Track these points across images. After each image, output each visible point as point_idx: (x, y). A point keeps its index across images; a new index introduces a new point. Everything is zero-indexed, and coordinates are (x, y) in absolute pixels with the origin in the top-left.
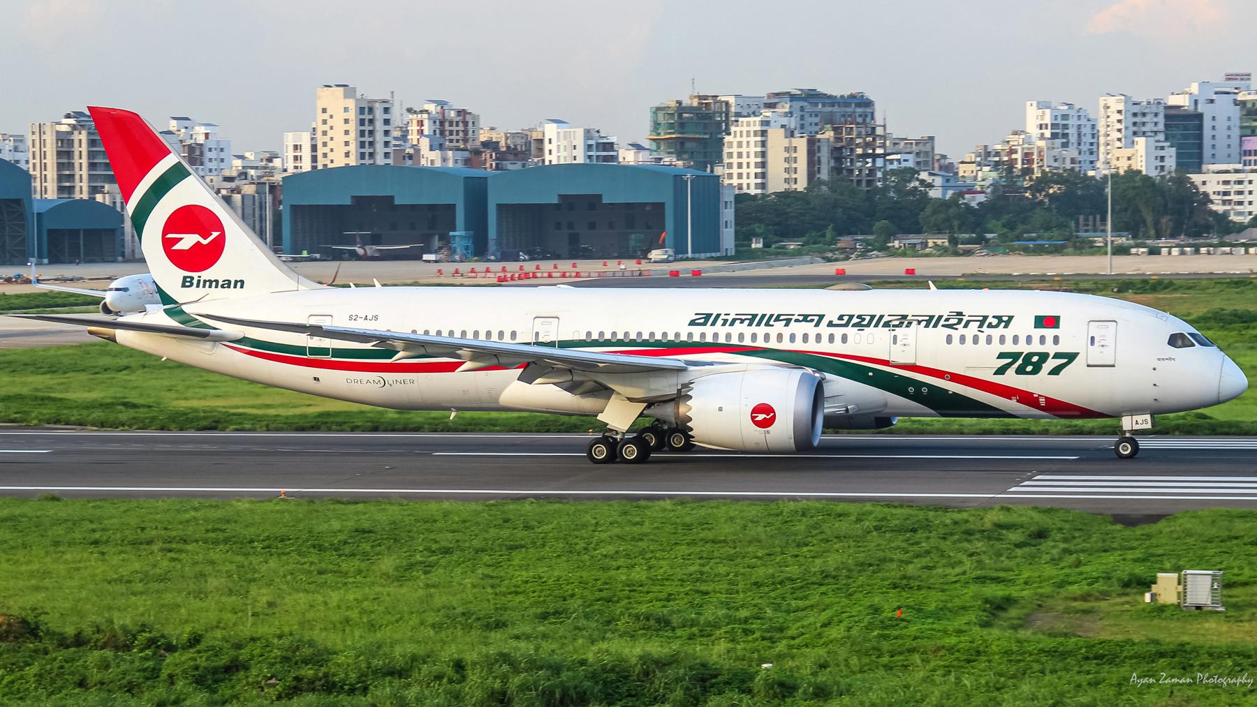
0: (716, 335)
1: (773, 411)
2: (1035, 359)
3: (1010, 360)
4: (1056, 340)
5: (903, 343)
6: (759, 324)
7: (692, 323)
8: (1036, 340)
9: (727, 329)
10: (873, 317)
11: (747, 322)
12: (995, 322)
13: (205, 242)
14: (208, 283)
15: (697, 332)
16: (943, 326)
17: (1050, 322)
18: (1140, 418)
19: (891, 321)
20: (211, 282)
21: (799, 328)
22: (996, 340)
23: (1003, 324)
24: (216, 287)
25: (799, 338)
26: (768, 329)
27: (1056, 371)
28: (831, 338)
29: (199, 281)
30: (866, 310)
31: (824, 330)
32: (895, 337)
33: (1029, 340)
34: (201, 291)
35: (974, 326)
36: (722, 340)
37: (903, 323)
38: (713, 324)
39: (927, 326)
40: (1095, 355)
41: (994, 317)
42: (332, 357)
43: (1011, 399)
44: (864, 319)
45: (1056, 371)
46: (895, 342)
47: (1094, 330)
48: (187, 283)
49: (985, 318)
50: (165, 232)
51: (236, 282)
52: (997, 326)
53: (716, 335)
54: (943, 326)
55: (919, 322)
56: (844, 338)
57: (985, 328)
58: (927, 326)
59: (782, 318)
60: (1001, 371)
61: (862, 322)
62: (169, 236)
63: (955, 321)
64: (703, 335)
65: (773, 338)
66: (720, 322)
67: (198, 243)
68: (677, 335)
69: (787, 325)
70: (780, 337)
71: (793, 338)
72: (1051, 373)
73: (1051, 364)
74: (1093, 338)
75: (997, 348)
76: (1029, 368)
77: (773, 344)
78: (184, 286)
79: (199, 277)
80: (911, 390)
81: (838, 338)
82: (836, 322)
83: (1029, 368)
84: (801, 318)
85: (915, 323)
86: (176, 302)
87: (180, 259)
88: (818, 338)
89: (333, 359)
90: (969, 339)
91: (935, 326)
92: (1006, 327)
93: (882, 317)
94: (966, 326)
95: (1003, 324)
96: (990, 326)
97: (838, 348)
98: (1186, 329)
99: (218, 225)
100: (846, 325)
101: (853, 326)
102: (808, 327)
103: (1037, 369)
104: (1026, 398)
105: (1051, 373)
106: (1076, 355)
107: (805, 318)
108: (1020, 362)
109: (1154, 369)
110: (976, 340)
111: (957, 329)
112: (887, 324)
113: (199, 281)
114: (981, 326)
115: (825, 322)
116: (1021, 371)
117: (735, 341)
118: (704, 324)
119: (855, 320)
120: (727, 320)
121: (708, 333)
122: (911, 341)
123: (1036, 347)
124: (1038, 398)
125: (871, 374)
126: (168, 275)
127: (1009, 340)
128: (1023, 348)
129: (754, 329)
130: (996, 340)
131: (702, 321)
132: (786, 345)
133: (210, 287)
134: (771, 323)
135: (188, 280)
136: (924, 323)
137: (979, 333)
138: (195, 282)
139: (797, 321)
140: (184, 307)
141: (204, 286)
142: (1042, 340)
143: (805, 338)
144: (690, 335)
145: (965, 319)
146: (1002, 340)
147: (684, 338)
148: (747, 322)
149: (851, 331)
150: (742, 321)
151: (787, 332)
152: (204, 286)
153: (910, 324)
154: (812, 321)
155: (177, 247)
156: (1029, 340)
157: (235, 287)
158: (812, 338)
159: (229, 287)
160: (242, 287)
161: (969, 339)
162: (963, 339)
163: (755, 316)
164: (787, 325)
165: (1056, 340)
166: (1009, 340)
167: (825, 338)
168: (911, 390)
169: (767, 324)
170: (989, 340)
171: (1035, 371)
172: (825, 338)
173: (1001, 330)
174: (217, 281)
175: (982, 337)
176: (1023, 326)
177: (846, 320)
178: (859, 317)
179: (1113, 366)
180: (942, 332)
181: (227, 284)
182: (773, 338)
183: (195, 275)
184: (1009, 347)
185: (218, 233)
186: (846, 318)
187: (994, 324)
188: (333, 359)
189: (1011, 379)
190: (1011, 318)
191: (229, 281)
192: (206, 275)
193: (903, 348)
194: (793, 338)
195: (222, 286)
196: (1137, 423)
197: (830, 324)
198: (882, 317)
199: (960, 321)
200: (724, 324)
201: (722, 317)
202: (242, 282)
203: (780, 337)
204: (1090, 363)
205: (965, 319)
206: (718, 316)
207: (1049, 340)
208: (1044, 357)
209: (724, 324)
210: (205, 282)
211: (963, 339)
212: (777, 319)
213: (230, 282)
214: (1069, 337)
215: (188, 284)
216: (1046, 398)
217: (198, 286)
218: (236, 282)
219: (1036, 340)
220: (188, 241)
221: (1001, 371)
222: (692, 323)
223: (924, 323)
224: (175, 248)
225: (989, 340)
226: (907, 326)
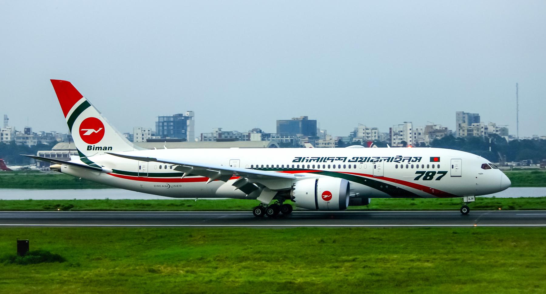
0: (303, 166)
1: (331, 195)
2: (430, 174)
3: (421, 174)
4: (439, 166)
5: (378, 168)
6: (321, 161)
7: (294, 161)
8: (431, 166)
9: (308, 163)
10: (366, 158)
11: (316, 161)
12: (414, 159)
13: (96, 132)
14: (97, 148)
15: (296, 165)
16: (394, 161)
17: (437, 159)
18: (470, 197)
19: (373, 160)
20: (99, 148)
22: (415, 166)
23: (418, 160)
24: (101, 150)
25: (337, 167)
26: (324, 163)
27: (439, 179)
28: (350, 167)
29: (94, 148)
31: (347, 163)
32: (375, 166)
33: (428, 166)
35: (406, 161)
36: (306, 168)
37: (378, 160)
38: (302, 161)
39: (388, 161)
40: (454, 172)
41: (414, 158)
42: (148, 176)
43: (421, 190)
44: (363, 159)
45: (439, 179)
46: (375, 168)
48: (89, 148)
49: (411, 158)
50: (81, 128)
51: (109, 148)
52: (415, 161)
53: (303, 166)
54: (394, 161)
55: (385, 160)
56: (355, 167)
57: (411, 162)
58: (388, 161)
59: (330, 159)
60: (417, 179)
62: (82, 130)
63: (399, 159)
64: (298, 166)
66: (305, 160)
68: (288, 166)
69: (332, 161)
70: (329, 167)
71: (334, 167)
72: (436, 180)
73: (436, 176)
74: (453, 166)
75: (415, 169)
76: (428, 178)
77: (326, 169)
78: (88, 149)
79: (94, 146)
81: (352, 167)
82: (352, 160)
83: (428, 178)
84: (338, 159)
85: (383, 160)
86: (85, 156)
87: (86, 139)
88: (345, 167)
90: (404, 167)
91: (391, 161)
92: (419, 161)
93: (370, 158)
94: (403, 161)
95: (418, 160)
96: (413, 161)
97: (352, 170)
98: (487, 162)
100: (356, 161)
101: (359, 161)
102: (341, 163)
103: (431, 178)
105: (436, 180)
106: (447, 172)
107: (339, 159)
108: (424, 175)
109: (476, 178)
110: (407, 167)
111: (400, 162)
112: (372, 161)
113: (94, 148)
114: (409, 161)
115: (347, 160)
116: (425, 179)
117: (311, 168)
118: (299, 161)
119: (359, 159)
120: (308, 160)
121: (301, 164)
122: (381, 168)
123: (431, 169)
126: (82, 146)
127: (420, 166)
128: (426, 170)
129: (319, 163)
130: (415, 166)
131: (298, 160)
132: (332, 170)
133: (98, 150)
134: (326, 161)
135: (90, 147)
136: (387, 160)
137: (408, 164)
138: (92, 148)
140: (88, 158)
141: (96, 150)
142: (433, 166)
143: (339, 167)
144: (293, 166)
145: (403, 158)
146: (418, 166)
147: (290, 167)
148: (316, 161)
149: (357, 164)
150: (314, 160)
151: (332, 165)
152: (96, 150)
153: (381, 161)
154: (342, 160)
155: (85, 134)
156: (428, 166)
158: (342, 167)
160: (111, 150)
161: (404, 167)
162: (402, 167)
164: (332, 161)
165: (439, 166)
166: (420, 166)
167: (347, 167)
168: (381, 187)
169: (324, 161)
170: (412, 167)
172: (347, 167)
173: (417, 163)
174: (101, 148)
175: (410, 166)
176: (425, 161)
177: (356, 159)
178: (361, 158)
179: (461, 176)
180: (394, 164)
181: (105, 148)
183: (92, 145)
184: (420, 169)
185: (102, 128)
186: (355, 159)
187: (414, 160)
189: (421, 182)
190: (421, 158)
191: (106, 148)
192: (97, 145)
194: (334, 167)
195: (103, 150)
196: (469, 199)
197: (349, 161)
198: (370, 158)
199: (401, 159)
200: (307, 161)
201: (306, 159)
202: (111, 148)
203: (329, 167)
204: (452, 175)
205: (403, 158)
206: (304, 158)
207: (436, 166)
208: (434, 173)
209: (307, 161)
210: (96, 148)
211: (402, 167)
212: (328, 159)
213: (106, 148)
214: (444, 166)
215: (89, 149)
216: (435, 189)
217: (93, 150)
218: (109, 148)
219: (431, 166)
220: (89, 132)
222: (294, 161)
225: (412, 167)
226: (380, 162)
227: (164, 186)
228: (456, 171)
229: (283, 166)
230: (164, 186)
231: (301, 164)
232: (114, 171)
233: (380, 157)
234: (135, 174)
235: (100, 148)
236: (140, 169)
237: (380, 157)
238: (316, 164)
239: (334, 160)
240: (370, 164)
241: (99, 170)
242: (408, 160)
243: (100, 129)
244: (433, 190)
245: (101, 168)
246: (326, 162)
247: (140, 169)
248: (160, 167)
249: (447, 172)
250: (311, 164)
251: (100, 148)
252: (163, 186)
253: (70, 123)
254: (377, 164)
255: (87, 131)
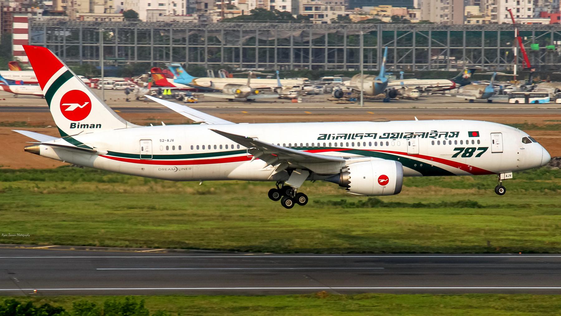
0: (330, 144)
2: (470, 150)
3: (459, 151)
4: (479, 142)
5: (413, 145)
6: (349, 138)
7: (319, 139)
8: (470, 142)
9: (335, 141)
10: (398, 134)
12: (452, 135)
13: (81, 107)
14: (83, 126)
16: (430, 137)
19: (406, 135)
20: (84, 125)
21: (367, 140)
22: (453, 142)
23: (455, 136)
24: (87, 127)
25: (367, 144)
26: (353, 141)
27: (479, 155)
28: (382, 144)
29: (78, 125)
30: (395, 131)
31: (378, 140)
32: (409, 142)
34: (80, 130)
35: (443, 137)
36: (333, 146)
38: (329, 139)
39: (423, 137)
40: (495, 148)
41: (451, 132)
42: (153, 159)
44: (395, 135)
45: (479, 155)
46: (409, 145)
47: (493, 137)
49: (447, 133)
50: (61, 103)
51: (97, 125)
52: (453, 136)
53: (330, 144)
54: (430, 137)
56: (387, 144)
58: (423, 137)
59: (358, 135)
60: (455, 156)
61: (394, 136)
63: (435, 135)
64: (324, 144)
65: (356, 144)
66: (331, 138)
67: (78, 107)
68: (313, 144)
69: (361, 138)
70: (359, 144)
71: (364, 144)
73: (477, 152)
74: (493, 141)
75: (454, 146)
76: (468, 155)
77: (356, 147)
78: (71, 127)
79: (79, 123)
80: (415, 165)
81: (384, 144)
82: (383, 136)
83: (468, 155)
84: (367, 135)
85: (417, 136)
88: (376, 144)
89: (153, 160)
90: (442, 143)
91: (426, 137)
92: (457, 137)
93: (402, 134)
94: (440, 137)
95: (455, 136)
96: (450, 136)
97: (384, 148)
99: (88, 99)
100: (388, 138)
101: (391, 138)
102: (371, 139)
104: (464, 167)
106: (487, 148)
107: (369, 135)
108: (464, 152)
109: (518, 153)
110: (444, 143)
111: (436, 138)
112: (405, 137)
113: (78, 125)
114: (446, 136)
115: (378, 137)
116: (464, 156)
117: (339, 146)
118: (325, 139)
119: (391, 136)
121: (327, 142)
122: (416, 144)
123: (470, 145)
124: (469, 167)
125: (399, 159)
126: (63, 123)
127: (459, 142)
128: (465, 146)
129: (347, 140)
130: (453, 142)
131: (323, 137)
132: (362, 148)
133: (84, 127)
134: (354, 137)
135: (73, 125)
137: (446, 140)
138: (77, 126)
139: (365, 136)
141: (81, 127)
143: (370, 144)
144: (319, 144)
146: (456, 142)
147: (316, 145)
149: (390, 140)
150: (341, 137)
151: (362, 142)
152: (81, 127)
153: (415, 137)
155: (67, 110)
157: (97, 127)
158: (373, 144)
159: (94, 127)
160: (100, 127)
161: (442, 143)
163: (346, 135)
164: (361, 138)
166: (459, 142)
167: (379, 144)
169: (353, 138)
170: (450, 143)
171: (470, 156)
172: (379, 144)
173: (454, 138)
174: (88, 125)
175: (447, 142)
176: (464, 136)
178: (392, 134)
179: (502, 152)
180: (430, 140)
182: (356, 144)
183: (77, 122)
184: (459, 146)
185: (88, 103)
186: (387, 135)
188: (153, 160)
189: (460, 159)
190: (458, 133)
191: (94, 125)
192: (82, 122)
193: (413, 147)
194: (364, 144)
195: (90, 127)
197: (380, 137)
198: (402, 134)
199: (437, 135)
201: (332, 135)
202: (100, 125)
203: (359, 144)
204: (493, 151)
206: (330, 135)
207: (476, 142)
208: (474, 149)
209: (333, 139)
210: (82, 125)
212: (357, 136)
213: (94, 125)
214: (484, 140)
215: (73, 127)
216: (473, 167)
217: (78, 127)
218: (97, 125)
219: (470, 142)
220: (73, 107)
221: (455, 156)
222: (319, 139)
223: (421, 136)
224: (67, 110)
225: (450, 143)
226: (414, 138)
227: (171, 169)
228: (498, 147)
229: (307, 144)
230: (171, 169)
231: (327, 142)
232: (110, 153)
233: (413, 133)
234: (137, 156)
235: (86, 126)
236: (142, 150)
237: (413, 133)
238: (344, 142)
239: (364, 136)
240: (404, 141)
241: (92, 152)
242: (445, 135)
243: (86, 103)
244: (471, 168)
245: (93, 149)
246: (355, 139)
247: (142, 150)
248: (167, 148)
249: (488, 148)
250: (340, 141)
251: (86, 126)
252: (169, 169)
253: (49, 96)
254: (411, 140)
255: (70, 106)
